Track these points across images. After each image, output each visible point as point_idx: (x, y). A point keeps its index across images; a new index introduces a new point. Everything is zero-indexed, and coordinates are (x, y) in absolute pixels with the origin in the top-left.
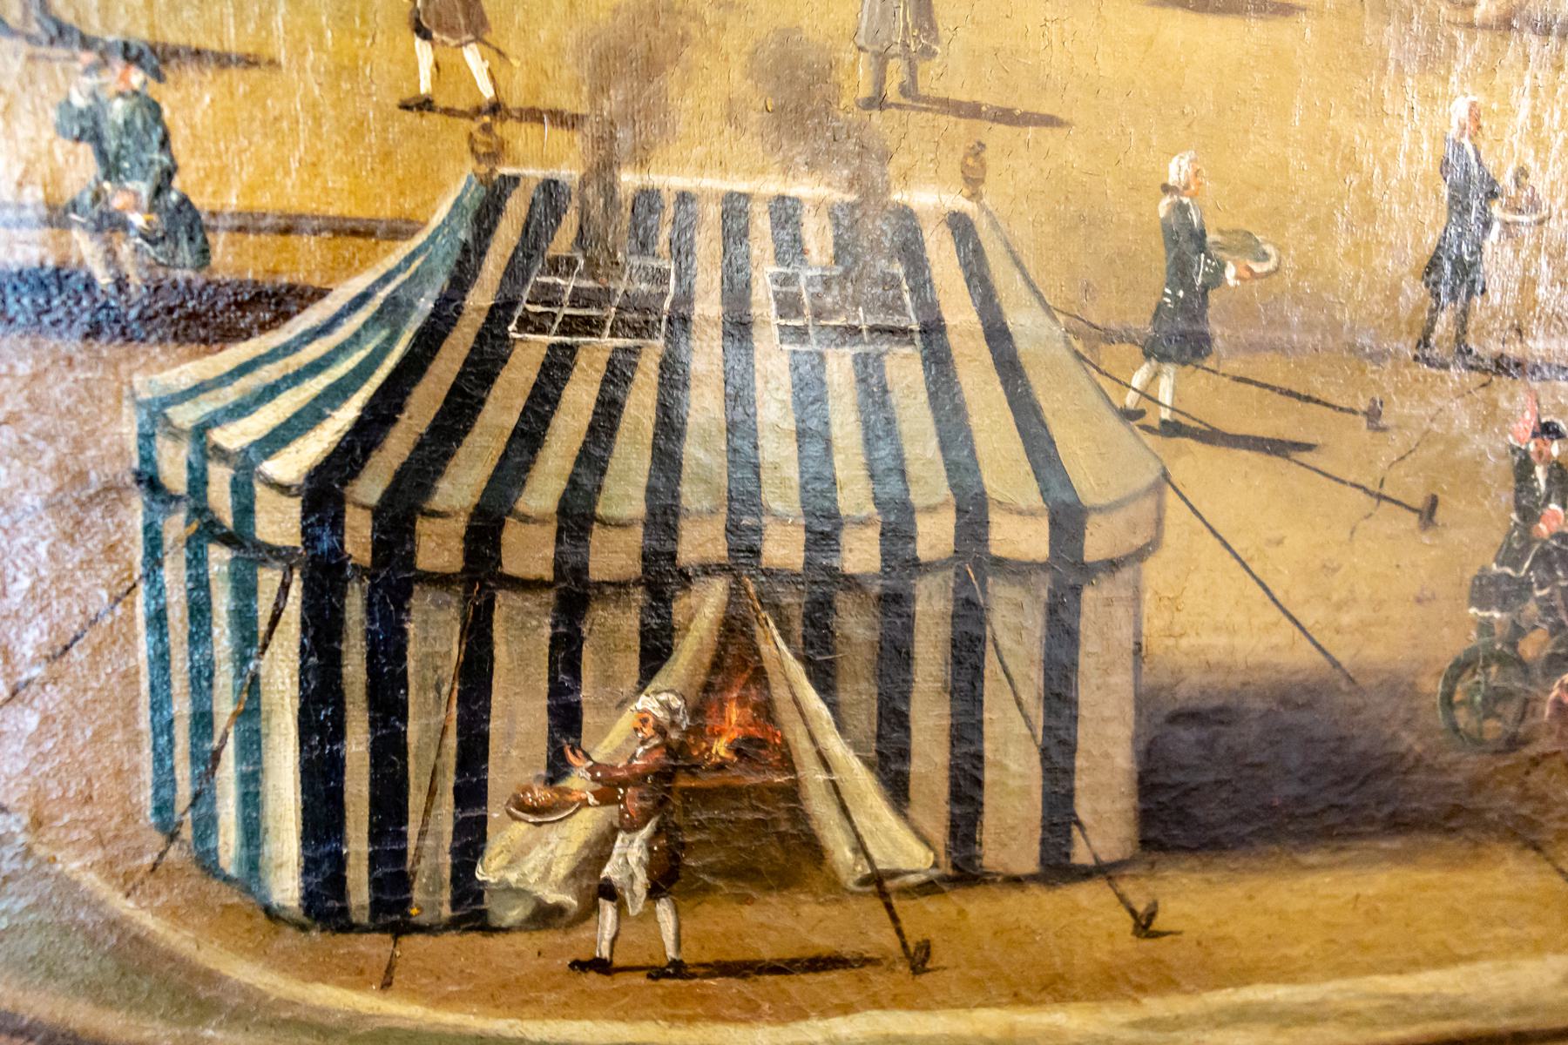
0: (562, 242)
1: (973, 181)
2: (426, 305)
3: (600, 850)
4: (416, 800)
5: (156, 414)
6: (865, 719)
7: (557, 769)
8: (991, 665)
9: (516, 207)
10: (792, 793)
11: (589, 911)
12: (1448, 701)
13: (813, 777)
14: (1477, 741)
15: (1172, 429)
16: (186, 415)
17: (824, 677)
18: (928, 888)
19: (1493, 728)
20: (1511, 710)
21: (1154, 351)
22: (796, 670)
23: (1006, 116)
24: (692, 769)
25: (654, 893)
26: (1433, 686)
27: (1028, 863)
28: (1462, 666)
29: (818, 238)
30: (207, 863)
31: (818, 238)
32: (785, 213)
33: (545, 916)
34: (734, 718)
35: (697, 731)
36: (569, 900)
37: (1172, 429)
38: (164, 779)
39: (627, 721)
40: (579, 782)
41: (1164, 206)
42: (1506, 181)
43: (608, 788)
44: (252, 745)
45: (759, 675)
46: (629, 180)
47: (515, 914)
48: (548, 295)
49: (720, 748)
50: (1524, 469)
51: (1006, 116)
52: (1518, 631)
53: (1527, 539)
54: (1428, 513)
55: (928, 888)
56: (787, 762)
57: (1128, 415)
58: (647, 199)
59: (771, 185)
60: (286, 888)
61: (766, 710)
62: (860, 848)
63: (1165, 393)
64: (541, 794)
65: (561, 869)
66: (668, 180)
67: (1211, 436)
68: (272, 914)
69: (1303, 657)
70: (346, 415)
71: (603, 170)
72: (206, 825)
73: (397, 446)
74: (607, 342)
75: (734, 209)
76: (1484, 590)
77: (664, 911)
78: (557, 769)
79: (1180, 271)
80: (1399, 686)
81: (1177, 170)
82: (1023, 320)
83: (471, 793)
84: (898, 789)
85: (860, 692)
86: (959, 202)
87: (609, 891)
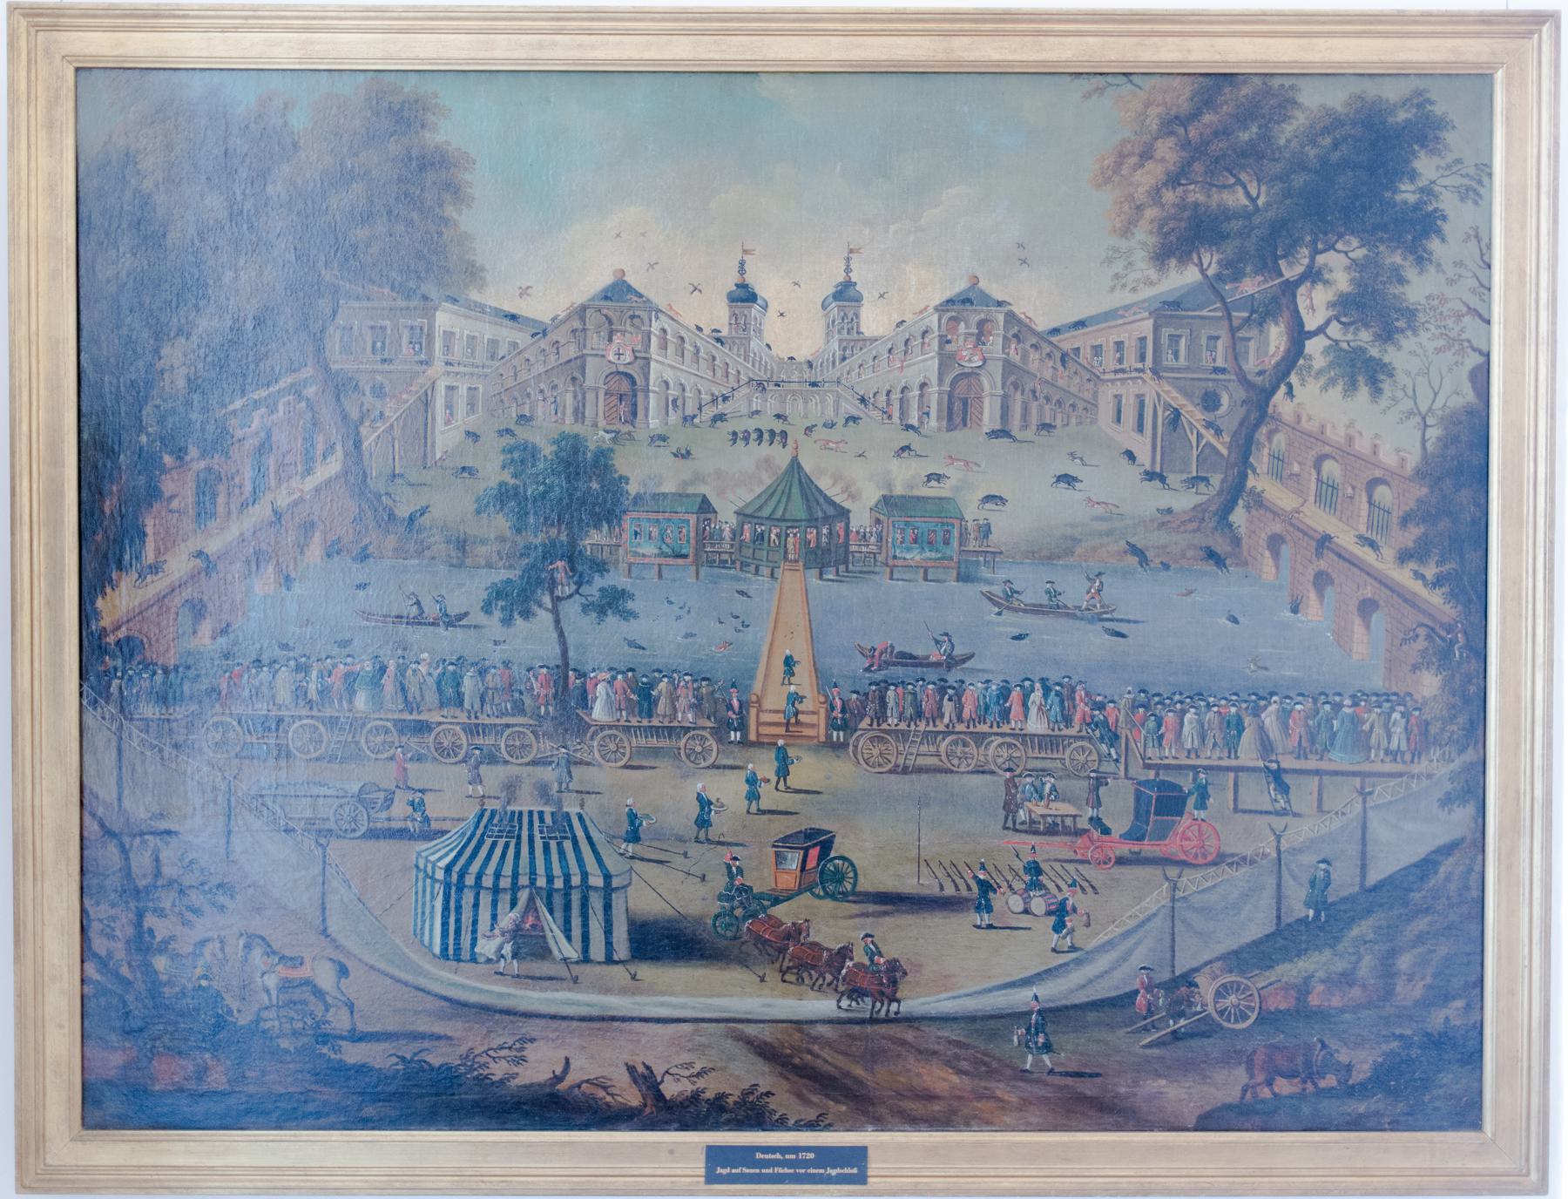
0: (495, 821)
1: (582, 806)
2: (469, 833)
3: (501, 948)
4: (463, 933)
5: (419, 854)
6: (560, 921)
7: (492, 928)
8: (591, 911)
9: (487, 815)
10: (544, 937)
11: (498, 961)
12: (714, 925)
13: (549, 935)
14: (724, 936)
15: (632, 858)
16: (424, 854)
17: (551, 911)
18: (577, 963)
19: (729, 934)
20: (734, 929)
21: (627, 840)
22: (545, 909)
23: (588, 793)
24: (521, 930)
25: (513, 958)
26: (709, 921)
27: (601, 958)
28: (717, 917)
29: (548, 820)
30: (422, 942)
31: (548, 820)
32: (541, 814)
33: (489, 961)
34: (531, 920)
35: (523, 921)
36: (494, 957)
37: (632, 858)
38: (416, 925)
39: (507, 919)
40: (497, 931)
41: (627, 809)
42: (714, 801)
43: (503, 934)
44: (432, 918)
45: (536, 910)
46: (509, 808)
47: (482, 959)
48: (492, 830)
49: (527, 926)
50: (729, 867)
51: (588, 793)
52: (733, 909)
53: (733, 885)
54: (703, 878)
55: (577, 963)
56: (542, 930)
57: (622, 854)
58: (513, 813)
59: (536, 809)
60: (437, 949)
61: (538, 918)
62: (560, 951)
63: (630, 849)
64: (488, 934)
65: (493, 950)
66: (517, 808)
67: (642, 859)
68: (434, 955)
69: (670, 912)
70: (453, 854)
71: (504, 808)
72: (423, 934)
73: (462, 861)
74: (504, 840)
75: (531, 813)
76: (721, 897)
77: (515, 961)
78: (492, 928)
79: (632, 823)
80: (699, 920)
81: (629, 802)
82: (594, 834)
83: (474, 931)
84: (569, 938)
85: (559, 914)
86: (578, 810)
87: (502, 956)
